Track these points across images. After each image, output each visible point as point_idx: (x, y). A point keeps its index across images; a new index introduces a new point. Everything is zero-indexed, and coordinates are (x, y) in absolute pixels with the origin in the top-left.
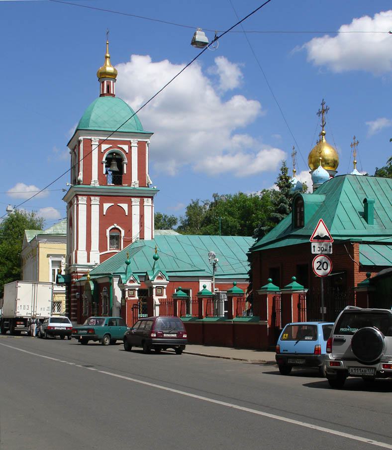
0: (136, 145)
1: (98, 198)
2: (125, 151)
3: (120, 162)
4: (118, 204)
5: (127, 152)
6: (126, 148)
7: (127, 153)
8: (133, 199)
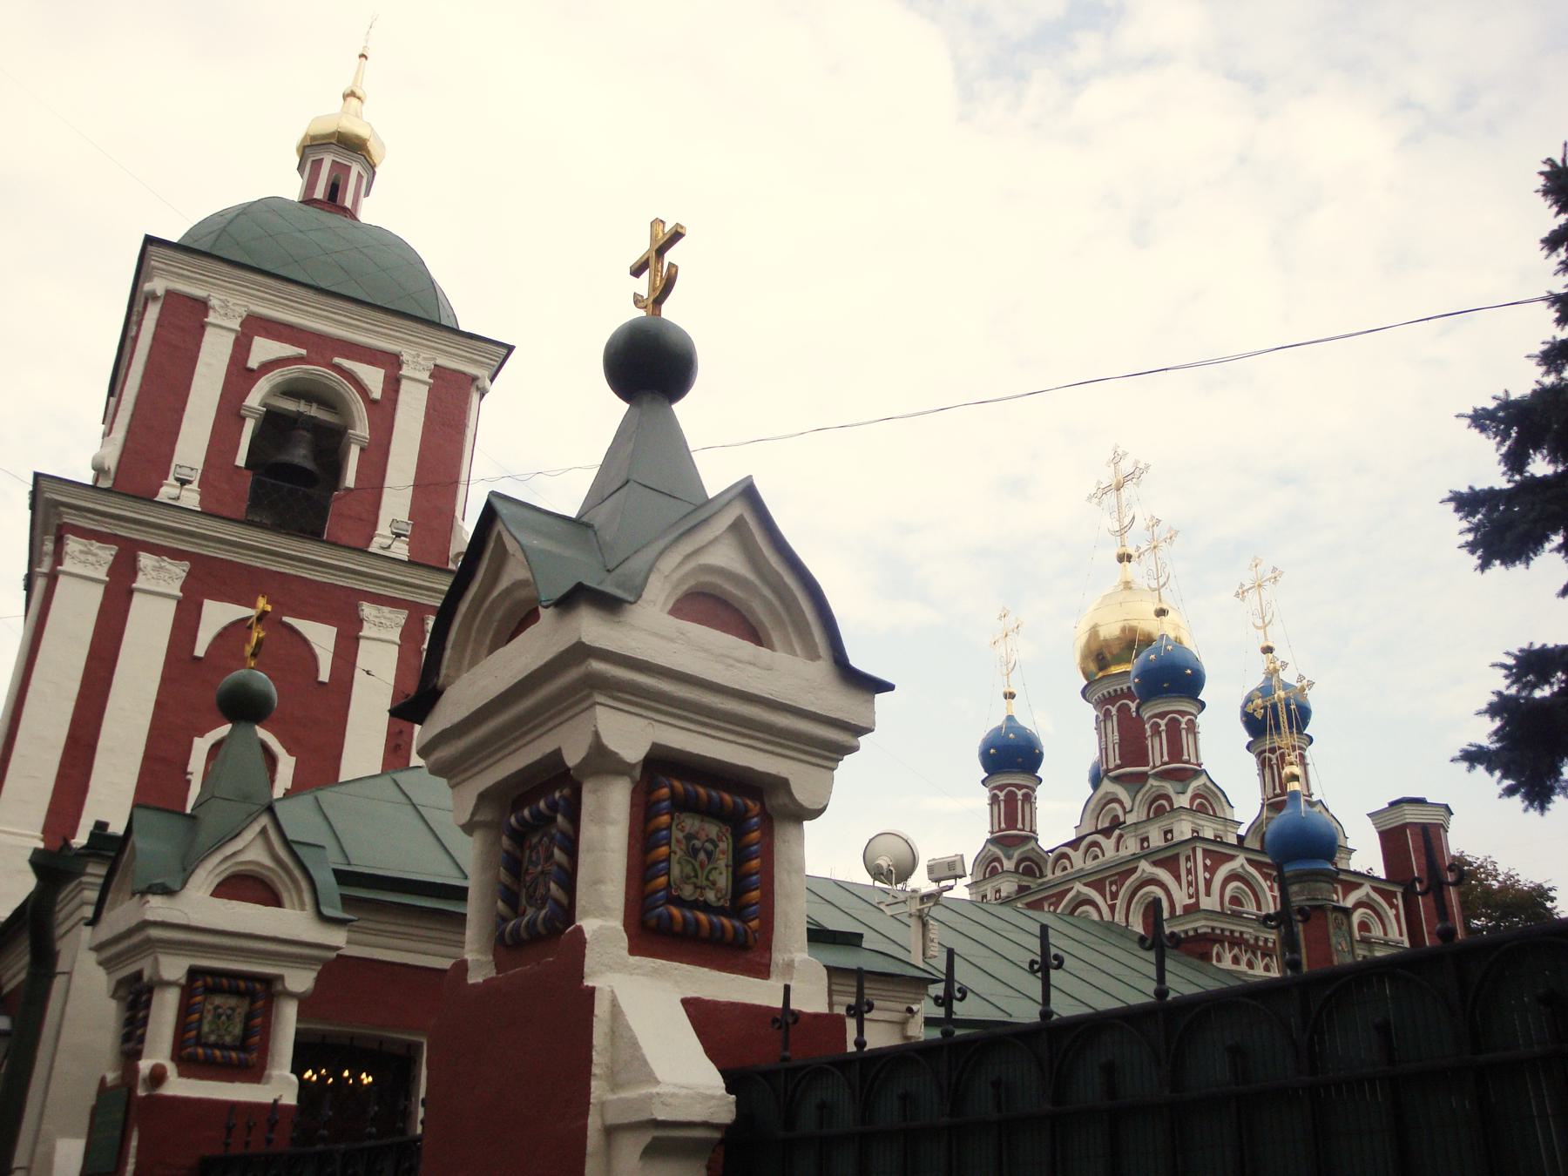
0: (425, 376)
1: (179, 570)
2: (363, 390)
3: (330, 442)
4: (286, 619)
5: (377, 394)
6: (373, 378)
7: (375, 402)
8: (368, 610)
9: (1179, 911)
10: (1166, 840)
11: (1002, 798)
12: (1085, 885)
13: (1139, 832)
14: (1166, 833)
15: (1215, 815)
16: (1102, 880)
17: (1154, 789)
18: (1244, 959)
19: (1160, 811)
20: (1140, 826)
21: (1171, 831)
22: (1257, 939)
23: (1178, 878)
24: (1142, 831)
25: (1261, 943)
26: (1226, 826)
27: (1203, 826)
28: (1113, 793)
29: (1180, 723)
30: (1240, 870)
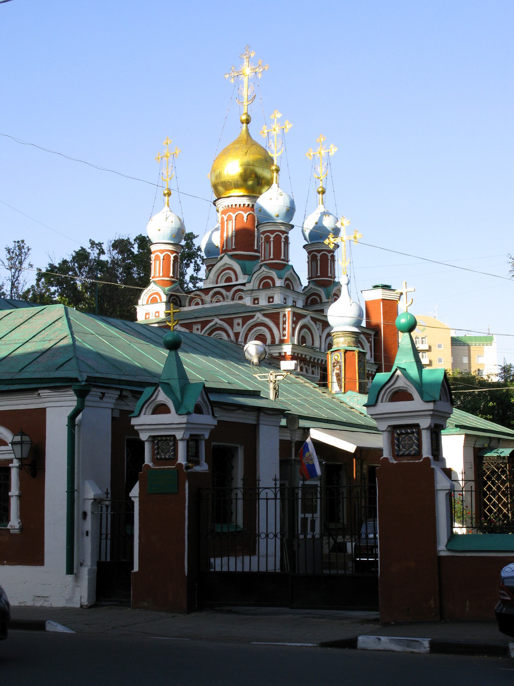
9: (277, 342)
10: (269, 302)
11: (162, 258)
12: (221, 320)
13: (253, 295)
14: (269, 298)
15: (293, 290)
16: (232, 319)
17: (264, 273)
18: (310, 371)
19: (266, 286)
20: (253, 292)
21: (273, 298)
22: (302, 355)
23: (277, 325)
24: (255, 294)
25: (312, 360)
26: (298, 296)
27: (288, 296)
28: (230, 265)
29: (281, 238)
30: (308, 323)
